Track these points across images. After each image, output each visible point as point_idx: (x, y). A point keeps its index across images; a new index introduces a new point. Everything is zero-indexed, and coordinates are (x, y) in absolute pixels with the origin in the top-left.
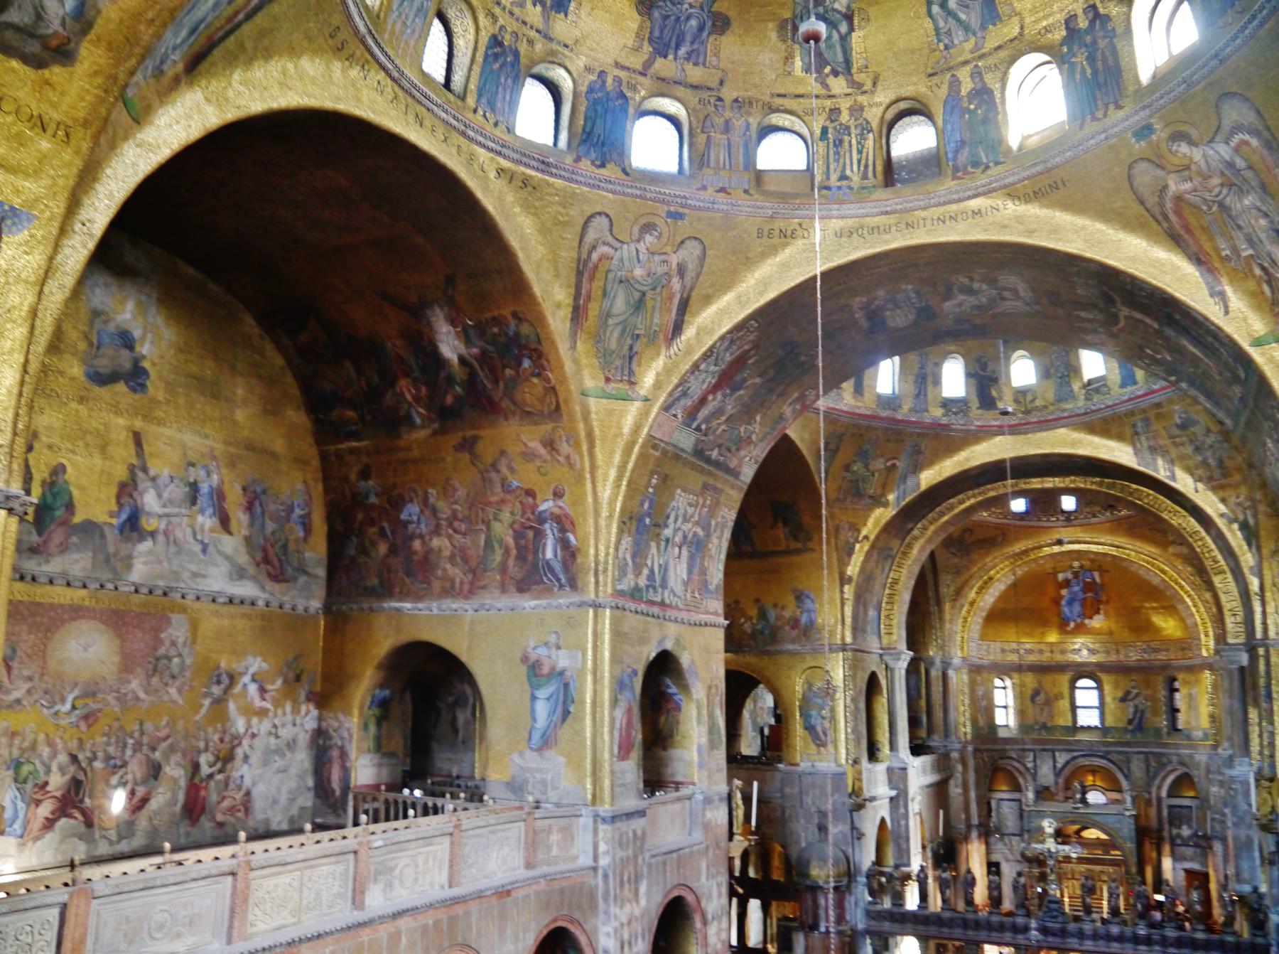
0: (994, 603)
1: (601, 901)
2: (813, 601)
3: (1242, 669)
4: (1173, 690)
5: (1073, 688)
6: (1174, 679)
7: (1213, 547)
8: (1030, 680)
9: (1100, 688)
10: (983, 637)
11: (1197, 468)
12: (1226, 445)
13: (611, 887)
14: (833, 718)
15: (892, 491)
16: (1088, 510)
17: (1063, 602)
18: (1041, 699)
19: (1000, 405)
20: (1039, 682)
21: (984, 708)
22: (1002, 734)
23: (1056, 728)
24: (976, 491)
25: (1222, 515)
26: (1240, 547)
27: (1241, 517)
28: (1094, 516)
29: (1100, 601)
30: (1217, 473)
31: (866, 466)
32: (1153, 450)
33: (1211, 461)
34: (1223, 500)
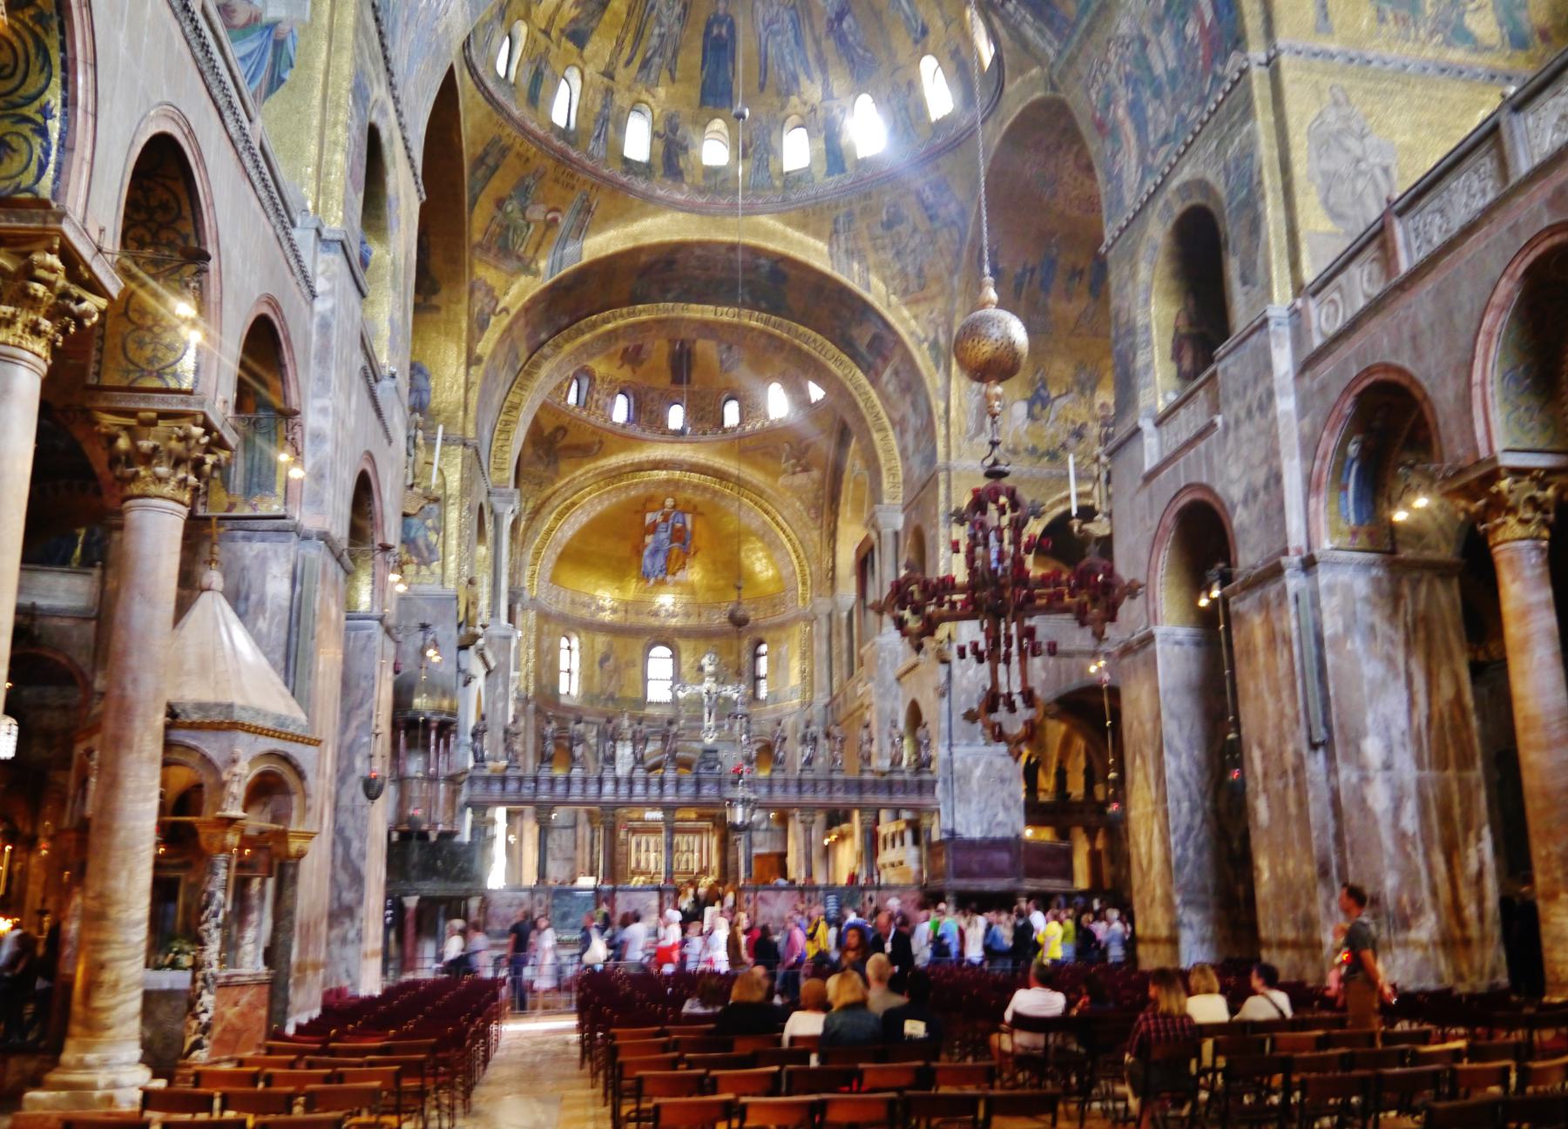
0: (572, 539)
1: (313, 362)
2: (427, 378)
3: (896, 534)
4: (756, 656)
5: (646, 657)
6: (761, 642)
7: (878, 402)
8: (601, 641)
9: (675, 656)
10: (554, 579)
11: (893, 278)
13: (334, 341)
14: (441, 529)
17: (646, 552)
18: (610, 664)
19: (688, 179)
20: (610, 645)
21: (547, 669)
22: (564, 701)
23: (624, 700)
24: (625, 310)
25: (912, 334)
27: (931, 337)
28: (705, 433)
29: (687, 554)
31: (523, 210)
32: (850, 254)
34: (916, 317)
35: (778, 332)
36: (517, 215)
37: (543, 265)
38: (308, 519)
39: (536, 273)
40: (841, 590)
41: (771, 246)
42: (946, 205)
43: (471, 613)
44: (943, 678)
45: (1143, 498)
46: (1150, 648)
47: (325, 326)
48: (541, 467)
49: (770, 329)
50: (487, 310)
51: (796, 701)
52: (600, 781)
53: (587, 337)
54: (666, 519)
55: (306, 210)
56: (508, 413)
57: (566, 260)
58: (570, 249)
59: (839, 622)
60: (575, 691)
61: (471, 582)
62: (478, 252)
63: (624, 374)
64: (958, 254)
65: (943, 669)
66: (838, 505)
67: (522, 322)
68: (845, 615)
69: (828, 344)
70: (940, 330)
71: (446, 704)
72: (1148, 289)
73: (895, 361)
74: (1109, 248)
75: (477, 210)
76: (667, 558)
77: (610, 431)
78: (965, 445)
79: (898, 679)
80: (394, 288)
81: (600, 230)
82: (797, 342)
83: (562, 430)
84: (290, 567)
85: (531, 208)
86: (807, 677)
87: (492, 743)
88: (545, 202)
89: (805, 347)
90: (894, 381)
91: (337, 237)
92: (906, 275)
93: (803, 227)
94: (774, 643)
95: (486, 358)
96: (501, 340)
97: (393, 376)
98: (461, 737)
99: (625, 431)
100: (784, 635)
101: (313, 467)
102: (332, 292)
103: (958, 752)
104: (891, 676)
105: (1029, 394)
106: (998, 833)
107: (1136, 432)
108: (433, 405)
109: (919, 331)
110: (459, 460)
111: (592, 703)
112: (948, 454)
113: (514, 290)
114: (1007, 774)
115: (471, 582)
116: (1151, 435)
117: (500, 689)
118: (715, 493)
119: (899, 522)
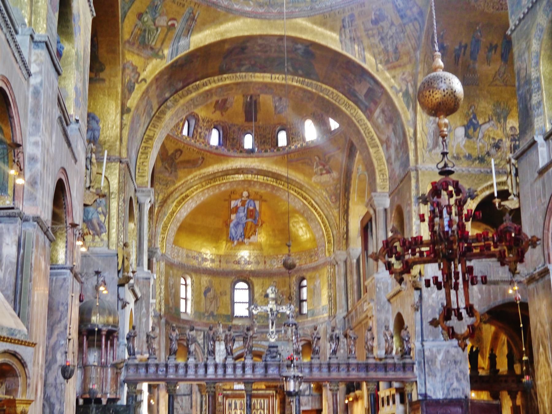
0: (187, 217)
1: (29, 115)
2: (97, 122)
3: (386, 210)
4: (300, 287)
5: (233, 289)
6: (303, 279)
7: (372, 130)
8: (205, 280)
9: (251, 289)
10: (175, 242)
11: (379, 54)
12: (402, 35)
13: (42, 102)
14: (107, 213)
15: (168, 47)
16: (263, 147)
18: (210, 294)
20: (210, 282)
22: (183, 317)
24: (216, 78)
25: (392, 87)
26: (403, 109)
27: (404, 88)
28: (266, 151)
29: (257, 225)
30: (392, 57)
31: (154, 20)
33: (390, 49)
34: (394, 77)
35: (309, 89)
36: (150, 23)
37: (166, 52)
38: (28, 210)
39: (162, 57)
40: (352, 246)
41: (304, 37)
42: (411, 9)
43: (126, 264)
44: (417, 299)
45: (538, 185)
46: (546, 278)
47: (36, 93)
48: (167, 174)
49: (305, 87)
50: (133, 80)
51: (326, 315)
52: (206, 366)
53: (194, 95)
54: (243, 204)
55: (24, 24)
56: (147, 141)
57: (180, 49)
58: (183, 42)
59: (351, 264)
60: (189, 311)
61: (125, 245)
62: (127, 45)
63: (217, 116)
64: (419, 38)
65: (416, 293)
66: (349, 193)
67: (154, 87)
68: (355, 261)
69: (341, 95)
70: (409, 85)
71: (111, 320)
72: (538, 56)
73: (382, 104)
74: (512, 31)
75: (126, 21)
76: (245, 229)
77: (208, 151)
78: (427, 155)
79: (389, 300)
80: (77, 69)
81: (200, 30)
82: (321, 94)
83: (179, 151)
84: (17, 238)
85: (159, 18)
86: (332, 300)
87: (139, 343)
88: (167, 14)
89: (327, 97)
90: (382, 116)
91: (43, 39)
92: (387, 51)
93: (323, 24)
94: (312, 279)
95: (132, 109)
96: (142, 98)
97: (77, 121)
98: (121, 340)
99: (218, 151)
100: (317, 274)
101: (31, 176)
102: (40, 72)
103: (427, 345)
104: (384, 299)
105: (466, 123)
106: (454, 396)
107: (534, 143)
108: (101, 138)
109: (396, 85)
110: (117, 171)
111: (200, 318)
112: (416, 161)
113: (149, 68)
114: (459, 358)
115: (125, 245)
116: (542, 146)
117: (144, 310)
118: (273, 187)
119: (387, 203)
